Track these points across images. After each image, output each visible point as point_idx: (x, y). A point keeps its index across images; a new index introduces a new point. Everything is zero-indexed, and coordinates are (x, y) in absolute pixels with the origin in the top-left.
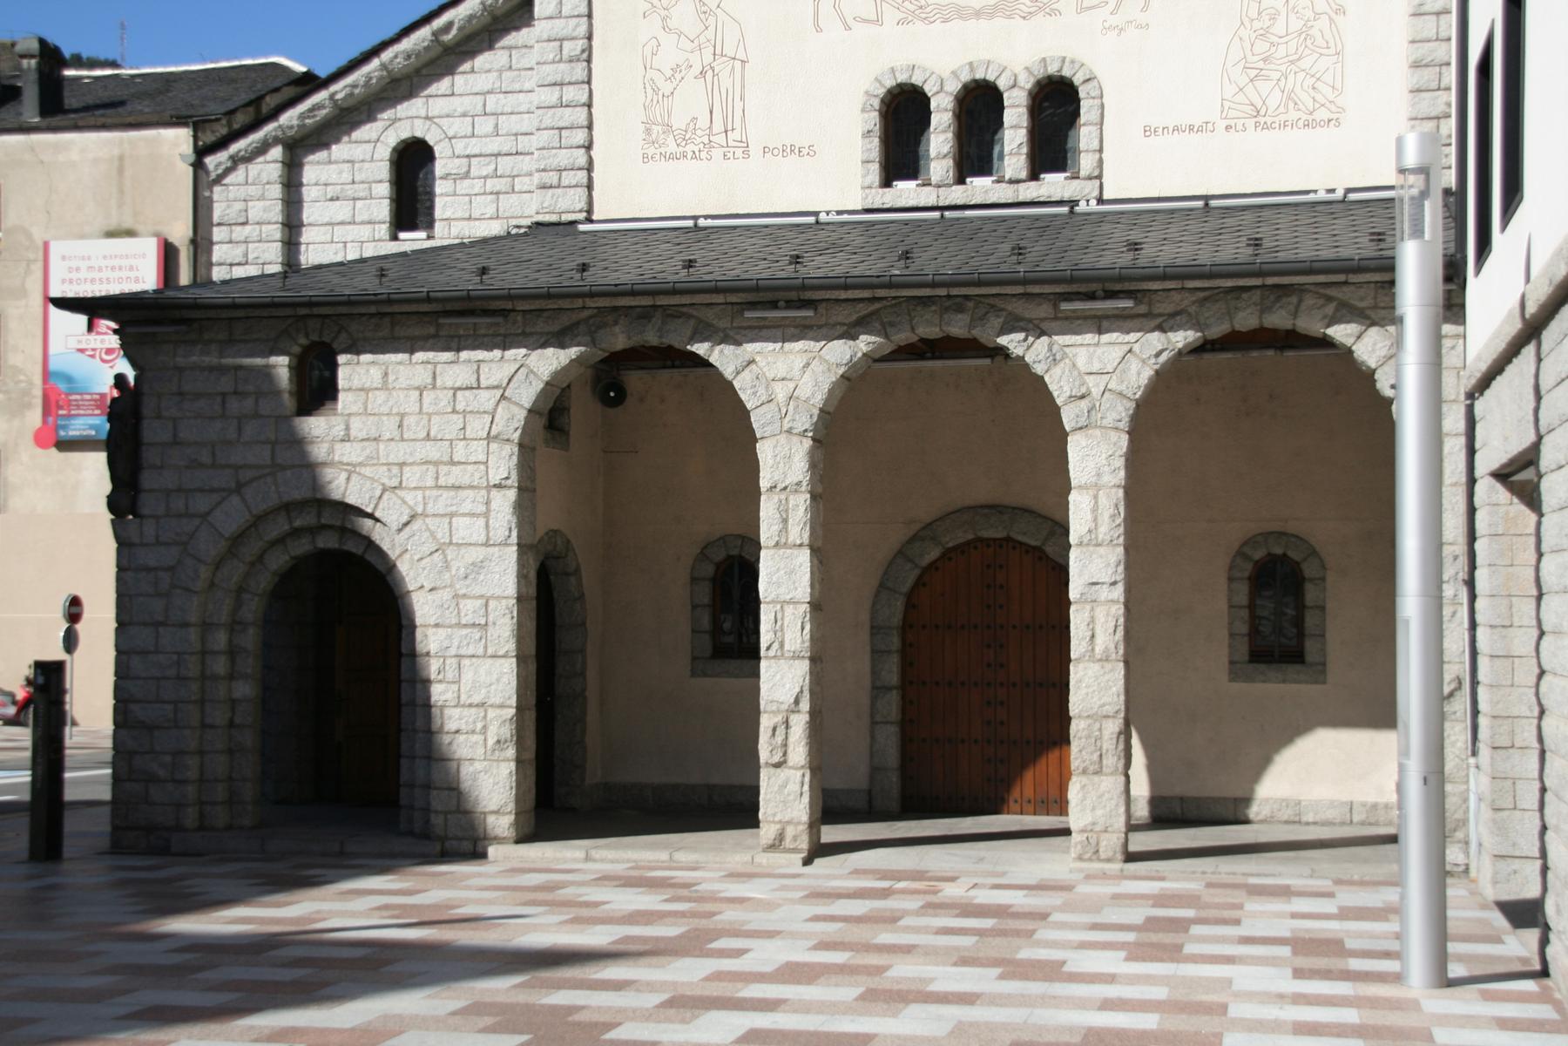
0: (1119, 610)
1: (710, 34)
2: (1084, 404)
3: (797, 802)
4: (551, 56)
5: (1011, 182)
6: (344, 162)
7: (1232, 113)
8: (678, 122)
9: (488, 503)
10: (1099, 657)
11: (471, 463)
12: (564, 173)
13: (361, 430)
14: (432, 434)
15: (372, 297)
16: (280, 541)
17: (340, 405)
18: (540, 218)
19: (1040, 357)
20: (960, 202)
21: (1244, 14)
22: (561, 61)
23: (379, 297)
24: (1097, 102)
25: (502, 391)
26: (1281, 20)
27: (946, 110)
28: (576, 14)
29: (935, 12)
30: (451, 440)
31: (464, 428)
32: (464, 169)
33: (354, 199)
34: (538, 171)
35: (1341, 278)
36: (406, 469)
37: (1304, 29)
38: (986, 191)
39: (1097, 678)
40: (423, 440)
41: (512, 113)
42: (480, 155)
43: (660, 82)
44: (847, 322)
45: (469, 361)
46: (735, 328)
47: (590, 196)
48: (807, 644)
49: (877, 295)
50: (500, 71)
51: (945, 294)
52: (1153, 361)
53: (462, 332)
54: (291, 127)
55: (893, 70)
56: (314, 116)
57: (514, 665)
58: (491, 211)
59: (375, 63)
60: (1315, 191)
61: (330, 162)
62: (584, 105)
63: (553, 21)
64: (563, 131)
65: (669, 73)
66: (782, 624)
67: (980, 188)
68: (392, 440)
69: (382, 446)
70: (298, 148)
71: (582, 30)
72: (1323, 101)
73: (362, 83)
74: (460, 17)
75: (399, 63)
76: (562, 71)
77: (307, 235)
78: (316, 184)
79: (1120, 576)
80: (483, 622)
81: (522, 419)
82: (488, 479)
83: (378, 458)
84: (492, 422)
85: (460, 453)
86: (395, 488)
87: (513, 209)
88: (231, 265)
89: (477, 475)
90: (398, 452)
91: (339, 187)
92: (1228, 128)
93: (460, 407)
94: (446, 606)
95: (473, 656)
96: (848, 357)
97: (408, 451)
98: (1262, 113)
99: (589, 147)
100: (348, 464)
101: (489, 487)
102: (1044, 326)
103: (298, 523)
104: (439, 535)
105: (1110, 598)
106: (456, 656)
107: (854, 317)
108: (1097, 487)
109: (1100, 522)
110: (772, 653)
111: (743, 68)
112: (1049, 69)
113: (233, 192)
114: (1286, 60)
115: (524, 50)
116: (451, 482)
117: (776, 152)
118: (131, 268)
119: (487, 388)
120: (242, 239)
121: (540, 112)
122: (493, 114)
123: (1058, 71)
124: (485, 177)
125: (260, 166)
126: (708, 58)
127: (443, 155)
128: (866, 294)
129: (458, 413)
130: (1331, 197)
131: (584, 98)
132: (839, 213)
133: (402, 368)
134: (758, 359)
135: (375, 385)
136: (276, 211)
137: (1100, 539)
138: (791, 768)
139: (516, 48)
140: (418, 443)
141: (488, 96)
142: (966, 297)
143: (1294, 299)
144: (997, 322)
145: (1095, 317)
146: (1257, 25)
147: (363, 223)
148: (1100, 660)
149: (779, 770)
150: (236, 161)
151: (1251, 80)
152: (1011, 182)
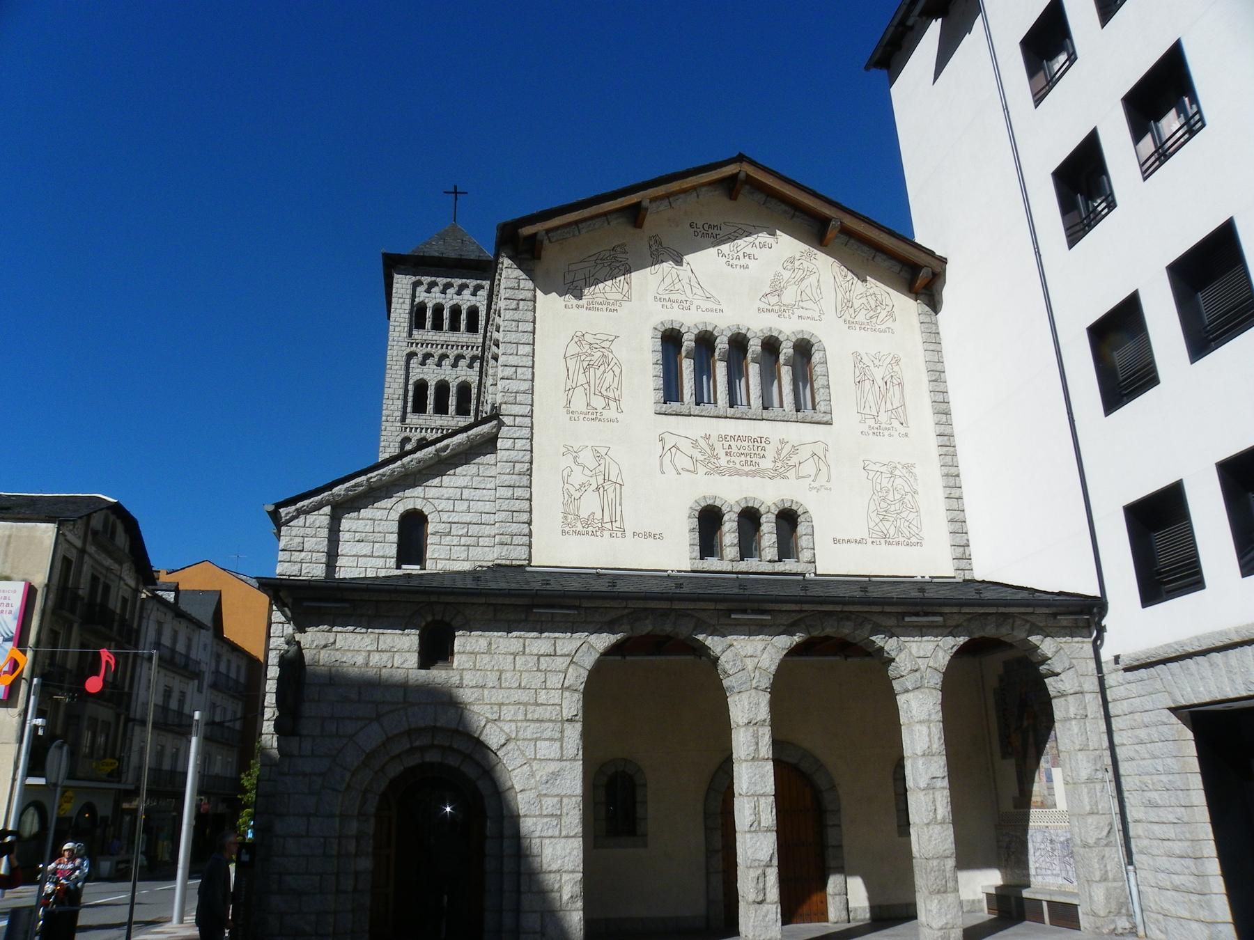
0: (946, 793)
1: (601, 468)
2: (918, 674)
3: (773, 927)
4: (508, 471)
5: (770, 561)
6: (368, 519)
7: (874, 536)
8: (584, 514)
9: (562, 732)
10: (939, 821)
11: (549, 705)
12: (515, 537)
13: (472, 680)
14: (523, 685)
15: (497, 591)
16: (399, 756)
17: (455, 664)
19: (893, 647)
20: (744, 570)
23: (501, 592)
24: (810, 524)
25: (571, 658)
26: (891, 492)
27: (734, 521)
30: (536, 689)
31: (545, 681)
32: (449, 530)
33: (374, 542)
34: (498, 534)
35: (1030, 610)
36: (504, 708)
38: (758, 566)
39: (939, 834)
40: (515, 688)
41: (478, 501)
42: (458, 523)
43: (572, 491)
44: (786, 623)
46: (722, 624)
47: (530, 552)
48: (775, 822)
49: (804, 609)
50: (472, 476)
52: (950, 651)
53: (543, 619)
54: (340, 495)
55: (705, 497)
56: (355, 490)
57: (581, 843)
58: (464, 556)
59: (399, 463)
61: (358, 519)
62: (527, 499)
63: (510, 451)
65: (578, 487)
66: (759, 810)
67: (751, 564)
68: (494, 687)
69: (486, 692)
70: (341, 509)
71: (527, 458)
72: (914, 533)
73: (388, 474)
75: (413, 465)
77: (341, 562)
78: (348, 531)
79: (946, 774)
80: (559, 813)
81: (586, 676)
82: (562, 716)
83: (483, 700)
84: (565, 678)
85: (542, 697)
86: (495, 720)
89: (554, 713)
90: (499, 696)
91: (364, 534)
92: (873, 542)
93: (543, 667)
94: (532, 802)
95: (552, 837)
96: (789, 644)
97: (505, 696)
98: (888, 537)
99: (530, 523)
101: (562, 721)
102: (893, 630)
103: (417, 743)
104: (527, 754)
105: (942, 786)
106: (539, 837)
107: (790, 621)
108: (929, 721)
109: (933, 742)
110: (753, 829)
111: (621, 489)
113: (295, 531)
114: (895, 512)
115: (487, 466)
116: (536, 716)
117: (640, 535)
118: (5, 598)
119: (561, 656)
120: (299, 560)
121: (501, 500)
124: (461, 536)
125: (315, 517)
127: (434, 521)
129: (541, 671)
130: (923, 580)
131: (528, 496)
132: (678, 571)
133: (501, 640)
134: (735, 643)
135: (482, 651)
136: (324, 545)
137: (934, 751)
138: (768, 903)
139: (482, 464)
140: (512, 690)
142: (851, 612)
143: (1011, 621)
144: (868, 627)
145: (917, 626)
146: (880, 494)
147: (378, 557)
148: (940, 823)
149: (761, 906)
150: (299, 513)
152: (770, 561)
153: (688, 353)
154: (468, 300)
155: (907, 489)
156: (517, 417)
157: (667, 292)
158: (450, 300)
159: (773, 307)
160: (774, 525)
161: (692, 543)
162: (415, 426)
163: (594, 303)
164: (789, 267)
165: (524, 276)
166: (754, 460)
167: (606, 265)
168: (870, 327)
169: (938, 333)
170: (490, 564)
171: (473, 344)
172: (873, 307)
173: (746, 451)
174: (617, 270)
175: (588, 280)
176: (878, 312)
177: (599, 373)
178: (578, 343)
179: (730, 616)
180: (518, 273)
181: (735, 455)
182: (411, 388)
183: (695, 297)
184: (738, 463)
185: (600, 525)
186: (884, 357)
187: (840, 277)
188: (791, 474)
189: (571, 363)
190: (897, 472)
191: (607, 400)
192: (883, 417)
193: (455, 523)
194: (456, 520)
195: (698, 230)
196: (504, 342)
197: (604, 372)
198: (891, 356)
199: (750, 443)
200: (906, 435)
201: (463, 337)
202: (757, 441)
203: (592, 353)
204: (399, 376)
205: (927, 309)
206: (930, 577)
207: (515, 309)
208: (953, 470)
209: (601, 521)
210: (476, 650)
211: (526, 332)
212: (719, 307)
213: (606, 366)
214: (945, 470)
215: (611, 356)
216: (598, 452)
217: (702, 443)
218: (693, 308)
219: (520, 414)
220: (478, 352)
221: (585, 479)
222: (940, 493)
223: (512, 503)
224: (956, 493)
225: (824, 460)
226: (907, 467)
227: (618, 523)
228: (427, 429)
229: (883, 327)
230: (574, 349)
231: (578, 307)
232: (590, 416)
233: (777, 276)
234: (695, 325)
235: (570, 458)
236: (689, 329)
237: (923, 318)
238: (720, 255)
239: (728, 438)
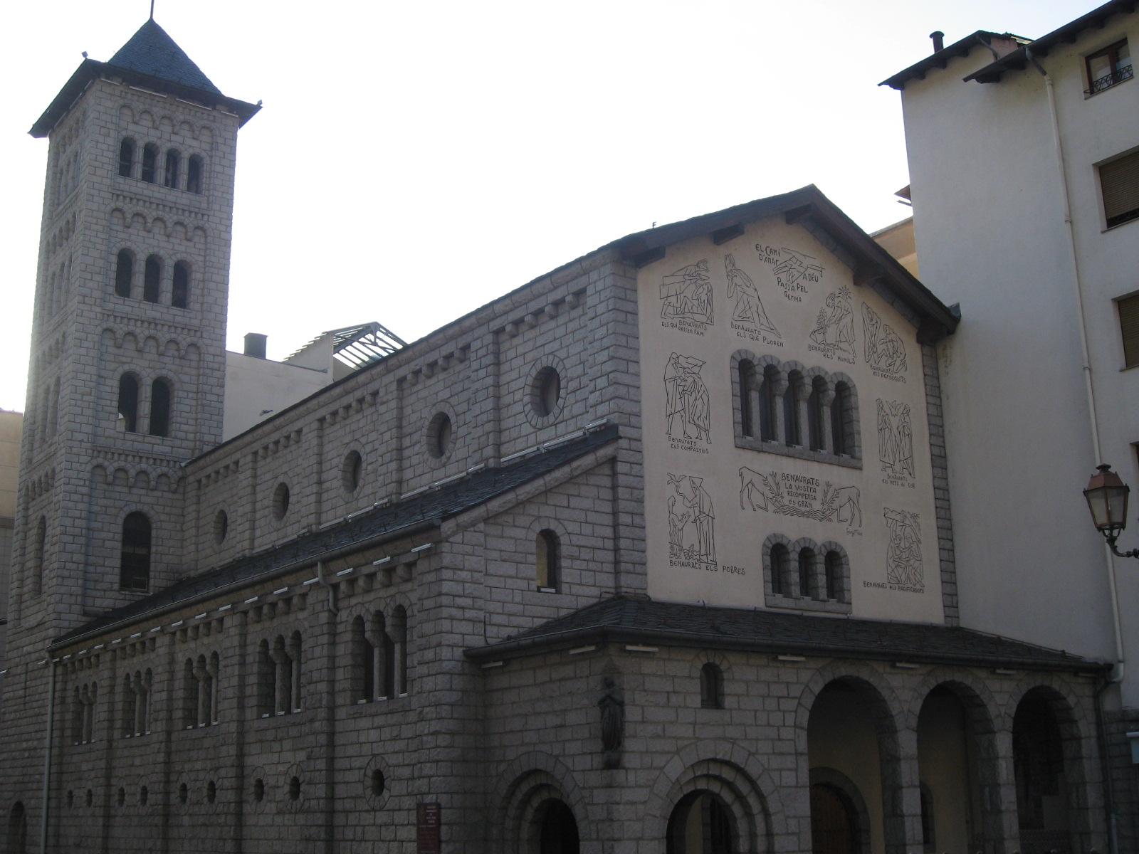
5: (821, 601)
8: (686, 547)
12: (636, 566)
22: (631, 500)
30: (778, 727)
43: (677, 523)
65: (680, 518)
80: (797, 831)
88: (454, 596)
100: (731, 739)
103: (699, 773)
104: (775, 781)
126: (697, 514)
154: (190, 146)
155: (914, 539)
158: (165, 139)
162: (121, 315)
164: (831, 304)
171: (197, 210)
172: (891, 354)
173: (802, 492)
174: (701, 290)
182: (114, 259)
183: (762, 326)
188: (834, 517)
189: (670, 386)
190: (907, 522)
192: (898, 467)
194: (582, 544)
195: (763, 254)
197: (696, 400)
201: (180, 197)
204: (100, 241)
212: (780, 340)
216: (694, 483)
217: (770, 479)
218: (761, 338)
220: (203, 222)
222: (934, 544)
224: (948, 545)
225: (856, 503)
226: (915, 516)
228: (136, 320)
229: (898, 375)
230: (671, 372)
231: (673, 325)
232: (686, 445)
234: (764, 357)
235: (673, 487)
238: (780, 283)
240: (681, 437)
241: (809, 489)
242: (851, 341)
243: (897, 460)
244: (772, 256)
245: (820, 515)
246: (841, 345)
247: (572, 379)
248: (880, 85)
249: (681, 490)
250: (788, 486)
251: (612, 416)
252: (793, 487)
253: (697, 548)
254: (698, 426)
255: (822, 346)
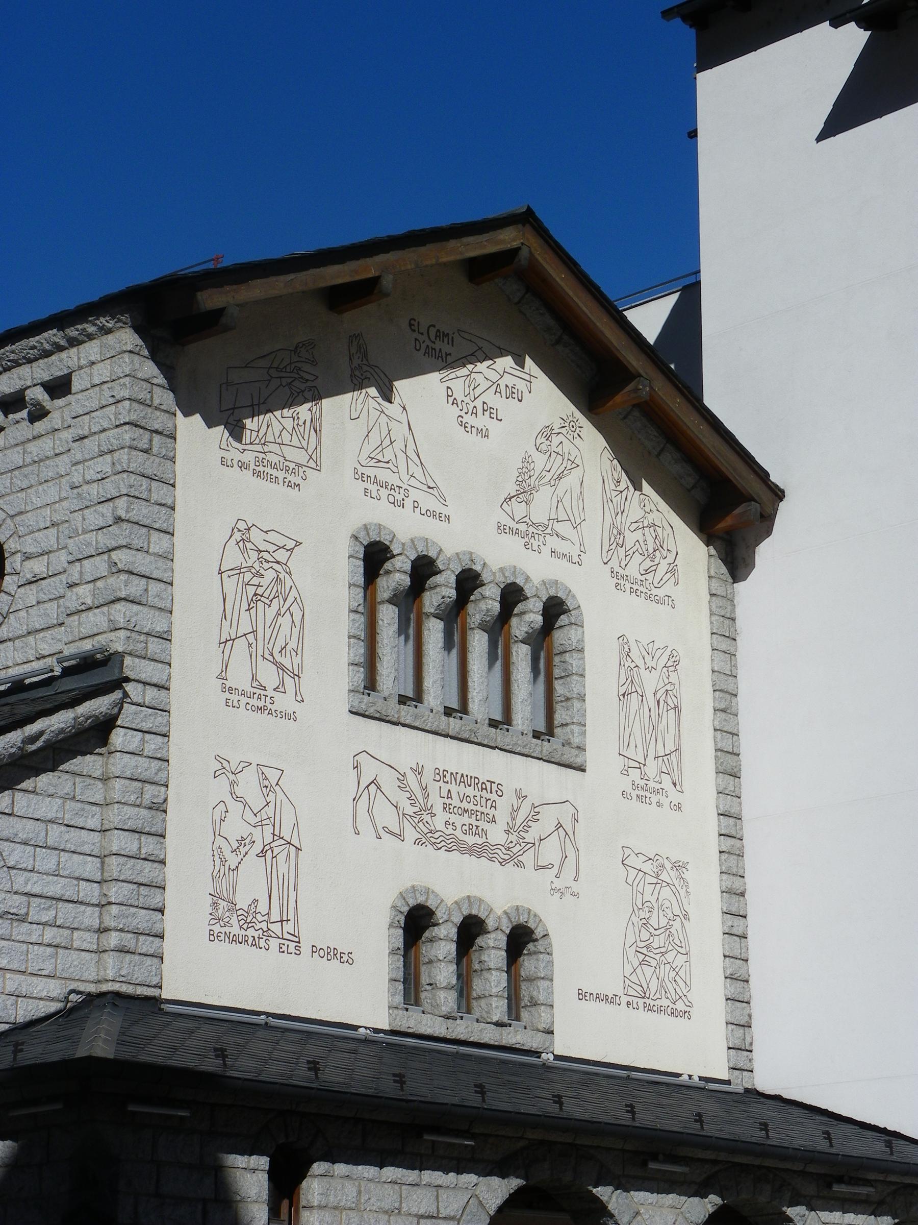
4: (133, 798)
7: (631, 992)
8: (243, 902)
12: (142, 938)
18: (116, 987)
21: (634, 902)
22: (138, 806)
26: (655, 912)
28: (159, 756)
29: (441, 838)
32: (23, 911)
37: (668, 927)
41: (73, 852)
42: (40, 896)
45: (429, 1185)
51: (801, 1168)
60: (680, 1075)
64: (142, 888)
65: (235, 846)
72: (681, 994)
74: (52, 729)
76: (140, 817)
87: (72, 969)
92: (628, 1003)
96: (702, 1217)
98: (647, 995)
111: (297, 856)
112: (521, 918)
115: (89, 781)
119: (445, 1218)
121: (122, 860)
122: (55, 849)
123: (526, 922)
124: (44, 924)
126: (269, 838)
128: (709, 1155)
133: (372, 1186)
135: (349, 1204)
141: (50, 826)
142: (768, 1168)
151: (640, 964)
153: (395, 595)
156: (147, 687)
157: (372, 463)
159: (519, 526)
160: (504, 954)
161: (394, 976)
163: (265, 464)
164: (544, 447)
165: (161, 380)
166: (483, 825)
167: (284, 382)
168: (644, 590)
169: (733, 620)
170: (92, 988)
172: (651, 550)
173: (470, 807)
175: (256, 408)
176: (656, 562)
177: (271, 612)
178: (241, 544)
179: (645, 1164)
180: (150, 369)
181: (456, 809)
183: (413, 482)
184: (459, 828)
185: (264, 925)
186: (660, 652)
187: (611, 481)
189: (230, 584)
190: (664, 876)
191: (281, 672)
192: (652, 768)
193: (35, 896)
194: (37, 890)
195: (421, 338)
196: (128, 521)
198: (668, 652)
199: (478, 794)
200: (679, 807)
202: (486, 789)
203: (262, 571)
205: (724, 570)
206: (701, 1078)
207: (146, 451)
208: (737, 884)
209: (266, 918)
210: (342, 1204)
211: (163, 505)
212: (444, 511)
213: (282, 602)
214: (728, 881)
215: (289, 583)
217: (411, 779)
218: (409, 503)
219: (155, 680)
221: (245, 831)
223: (138, 867)
225: (570, 833)
226: (679, 866)
227: (291, 923)
229: (661, 593)
231: (243, 466)
232: (254, 702)
233: (527, 460)
234: (412, 541)
236: (403, 549)
237: (716, 586)
239: (448, 779)
240: (245, 684)
241: (484, 800)
242: (578, 521)
243: (651, 755)
244: (438, 345)
245: (501, 854)
246: (558, 527)
247: (28, 557)
248: (667, 14)
249: (239, 791)
250: (444, 794)
251: (112, 636)
252: (454, 795)
253: (263, 907)
254: (280, 666)
255: (523, 527)
